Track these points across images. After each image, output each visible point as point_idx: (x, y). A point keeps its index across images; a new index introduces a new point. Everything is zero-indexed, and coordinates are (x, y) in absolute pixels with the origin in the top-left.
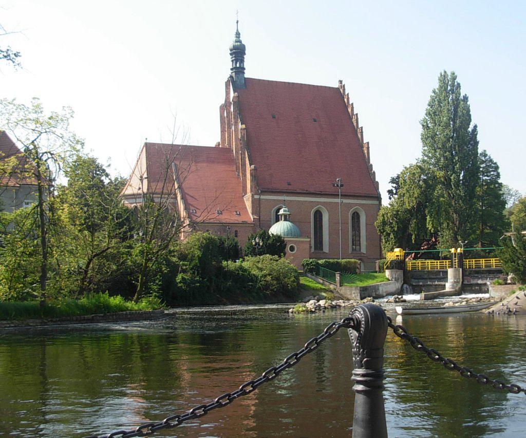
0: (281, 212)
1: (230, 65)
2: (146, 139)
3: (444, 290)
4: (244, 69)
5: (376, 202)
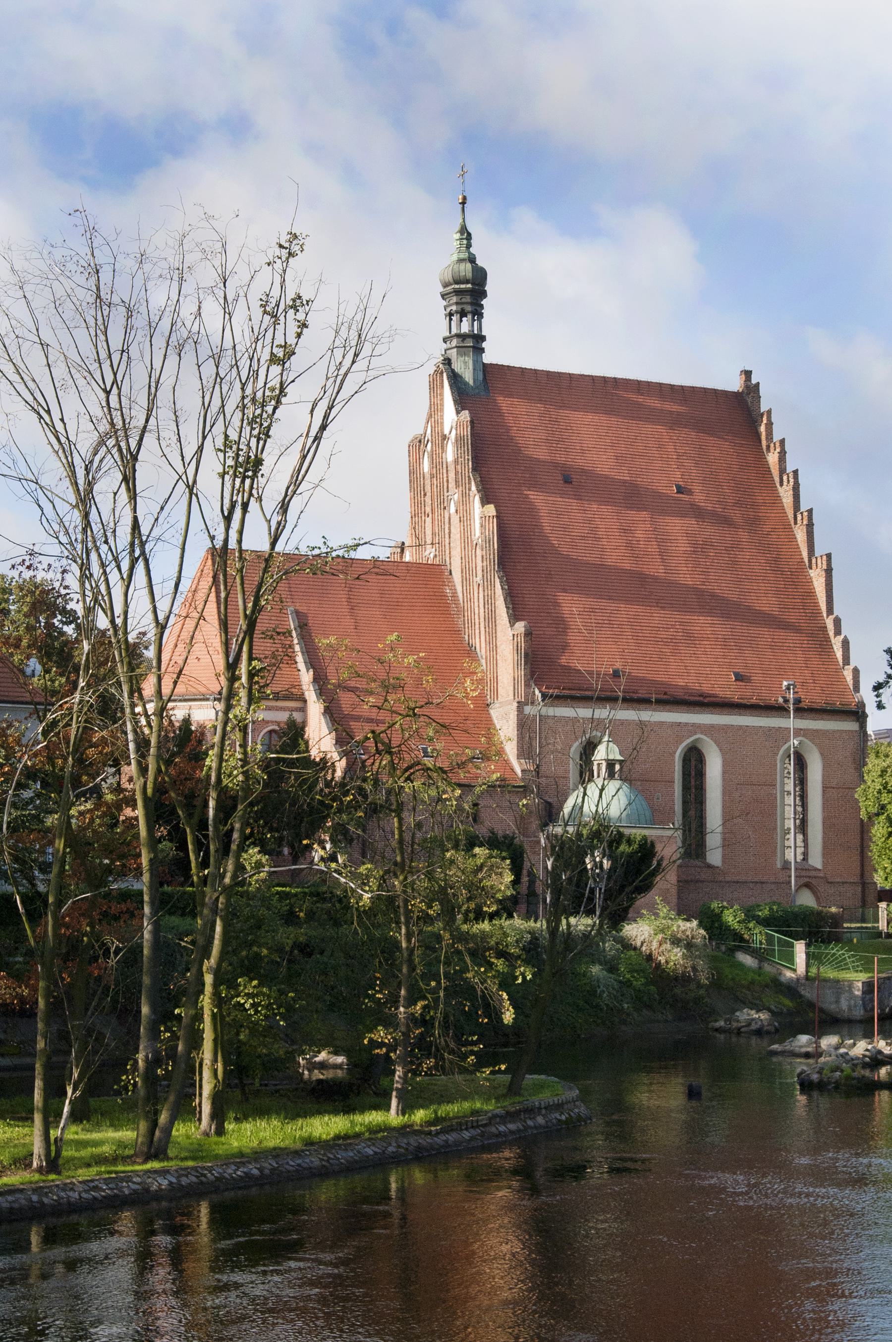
0: (600, 754)
4: (483, 338)
5: (851, 726)
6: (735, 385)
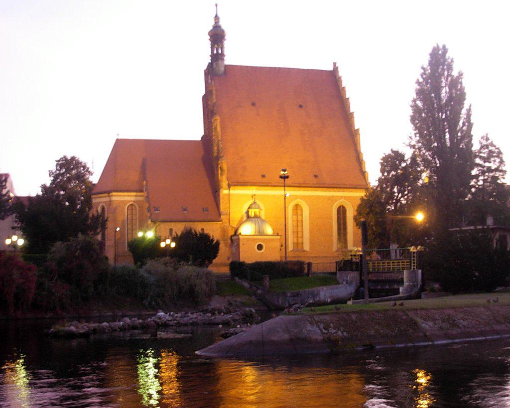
1: (208, 52)
2: (118, 135)
3: (397, 294)
6: (331, 68)
